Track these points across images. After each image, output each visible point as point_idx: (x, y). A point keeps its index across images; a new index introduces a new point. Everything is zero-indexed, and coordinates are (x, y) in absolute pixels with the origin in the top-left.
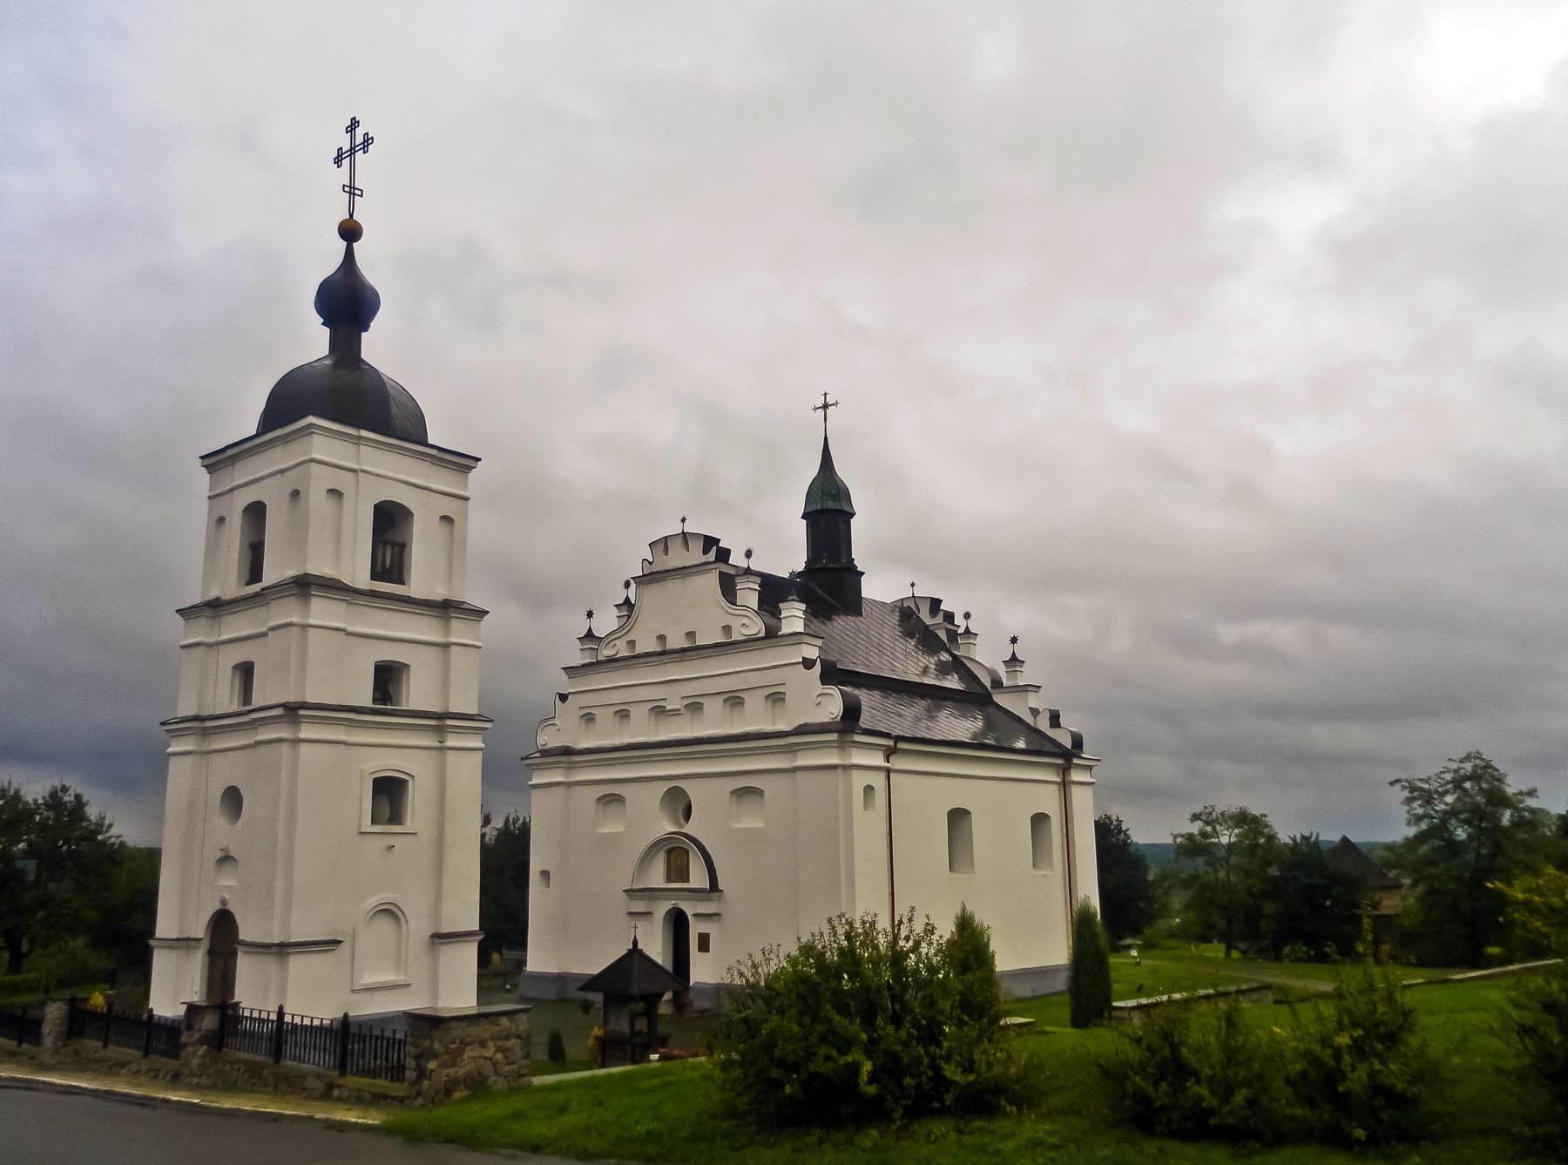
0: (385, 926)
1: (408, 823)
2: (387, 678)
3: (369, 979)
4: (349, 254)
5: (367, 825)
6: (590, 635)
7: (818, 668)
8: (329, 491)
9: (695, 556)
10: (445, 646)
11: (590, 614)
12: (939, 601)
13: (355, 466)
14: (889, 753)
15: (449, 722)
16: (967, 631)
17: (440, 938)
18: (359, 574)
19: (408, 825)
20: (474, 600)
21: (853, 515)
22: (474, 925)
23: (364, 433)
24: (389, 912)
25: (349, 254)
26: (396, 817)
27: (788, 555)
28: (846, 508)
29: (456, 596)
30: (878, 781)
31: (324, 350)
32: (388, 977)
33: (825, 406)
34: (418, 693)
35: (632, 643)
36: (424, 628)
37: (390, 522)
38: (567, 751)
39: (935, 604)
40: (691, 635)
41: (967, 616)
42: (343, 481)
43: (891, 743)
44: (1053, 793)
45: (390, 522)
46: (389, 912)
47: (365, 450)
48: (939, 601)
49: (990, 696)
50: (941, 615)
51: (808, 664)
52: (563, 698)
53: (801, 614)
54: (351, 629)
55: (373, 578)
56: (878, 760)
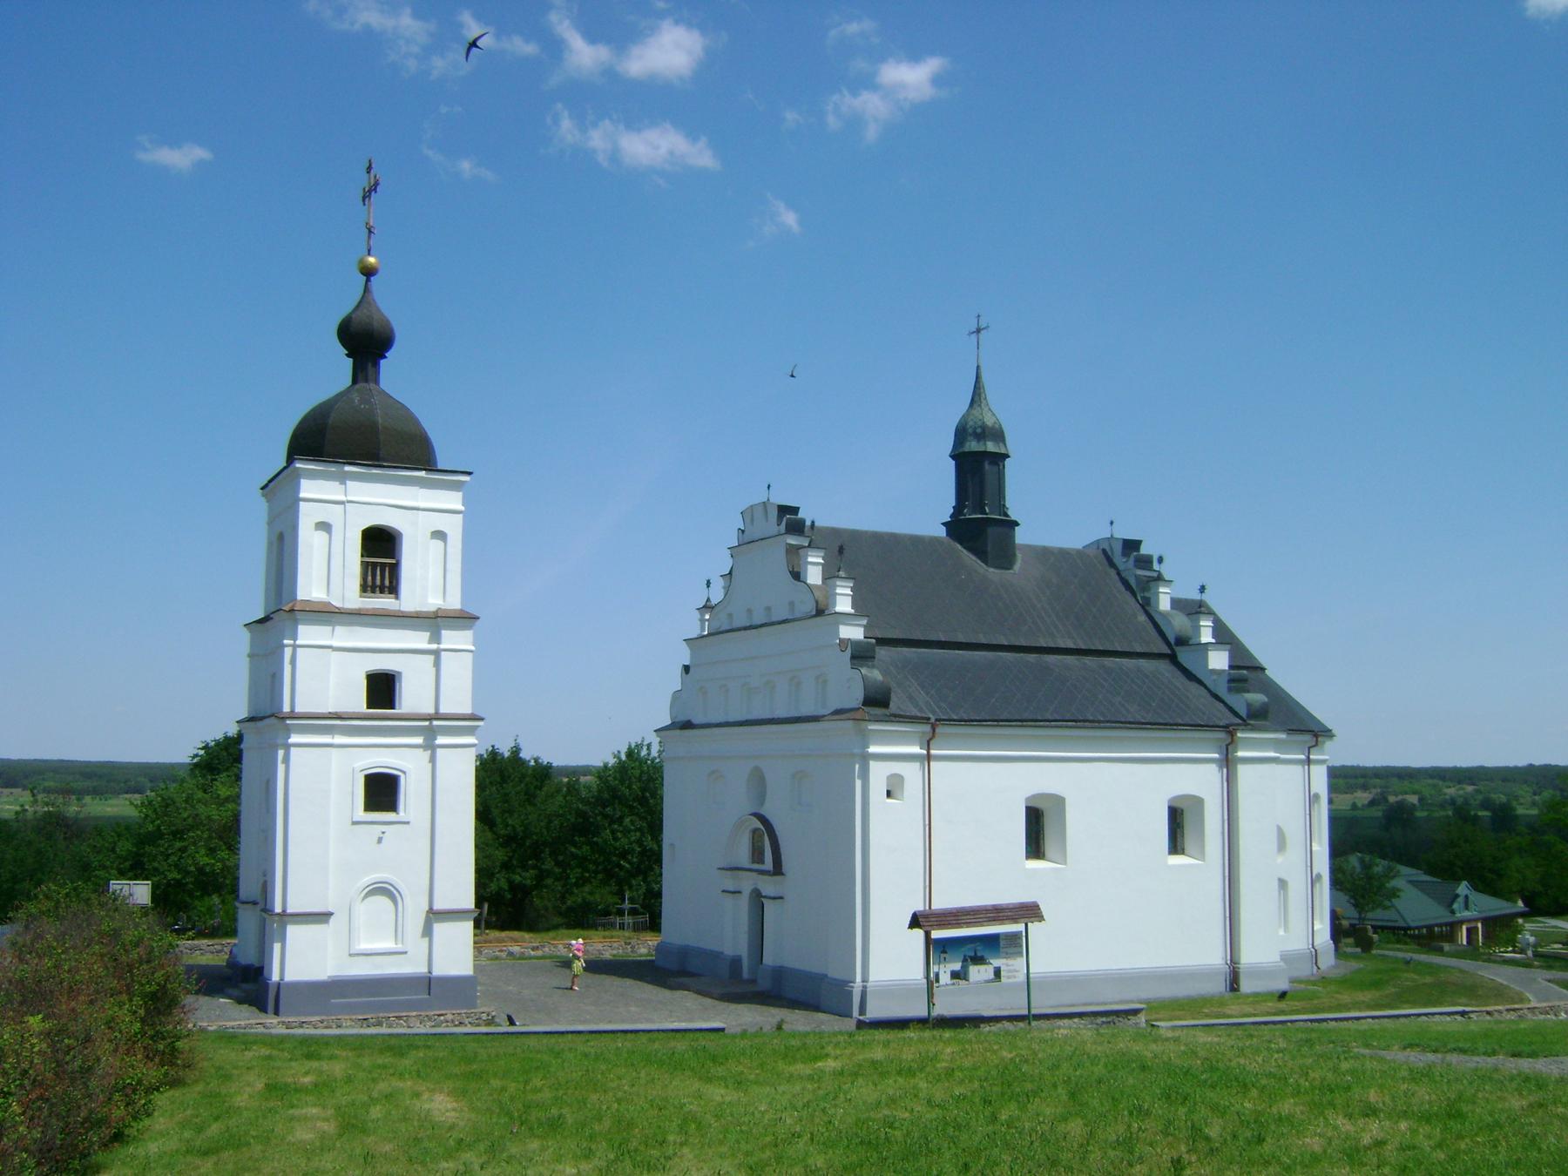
0: (382, 902)
1: (402, 813)
3: (364, 946)
4: (367, 289)
5: (360, 814)
6: (708, 607)
7: (848, 653)
9: (772, 525)
11: (708, 583)
13: (342, 498)
15: (435, 723)
16: (1159, 578)
17: (435, 915)
18: (349, 594)
19: (402, 815)
21: (1007, 456)
22: (467, 900)
23: (348, 468)
24: (383, 890)
27: (923, 504)
28: (991, 447)
30: (911, 772)
31: (347, 380)
32: (389, 945)
33: (978, 331)
34: (413, 696)
35: (730, 615)
36: (418, 639)
37: (380, 545)
38: (687, 725)
39: (1131, 546)
40: (768, 609)
41: (1160, 560)
42: (333, 514)
43: (927, 728)
45: (380, 545)
46: (383, 890)
51: (844, 643)
52: (687, 669)
53: (849, 592)
54: (335, 644)
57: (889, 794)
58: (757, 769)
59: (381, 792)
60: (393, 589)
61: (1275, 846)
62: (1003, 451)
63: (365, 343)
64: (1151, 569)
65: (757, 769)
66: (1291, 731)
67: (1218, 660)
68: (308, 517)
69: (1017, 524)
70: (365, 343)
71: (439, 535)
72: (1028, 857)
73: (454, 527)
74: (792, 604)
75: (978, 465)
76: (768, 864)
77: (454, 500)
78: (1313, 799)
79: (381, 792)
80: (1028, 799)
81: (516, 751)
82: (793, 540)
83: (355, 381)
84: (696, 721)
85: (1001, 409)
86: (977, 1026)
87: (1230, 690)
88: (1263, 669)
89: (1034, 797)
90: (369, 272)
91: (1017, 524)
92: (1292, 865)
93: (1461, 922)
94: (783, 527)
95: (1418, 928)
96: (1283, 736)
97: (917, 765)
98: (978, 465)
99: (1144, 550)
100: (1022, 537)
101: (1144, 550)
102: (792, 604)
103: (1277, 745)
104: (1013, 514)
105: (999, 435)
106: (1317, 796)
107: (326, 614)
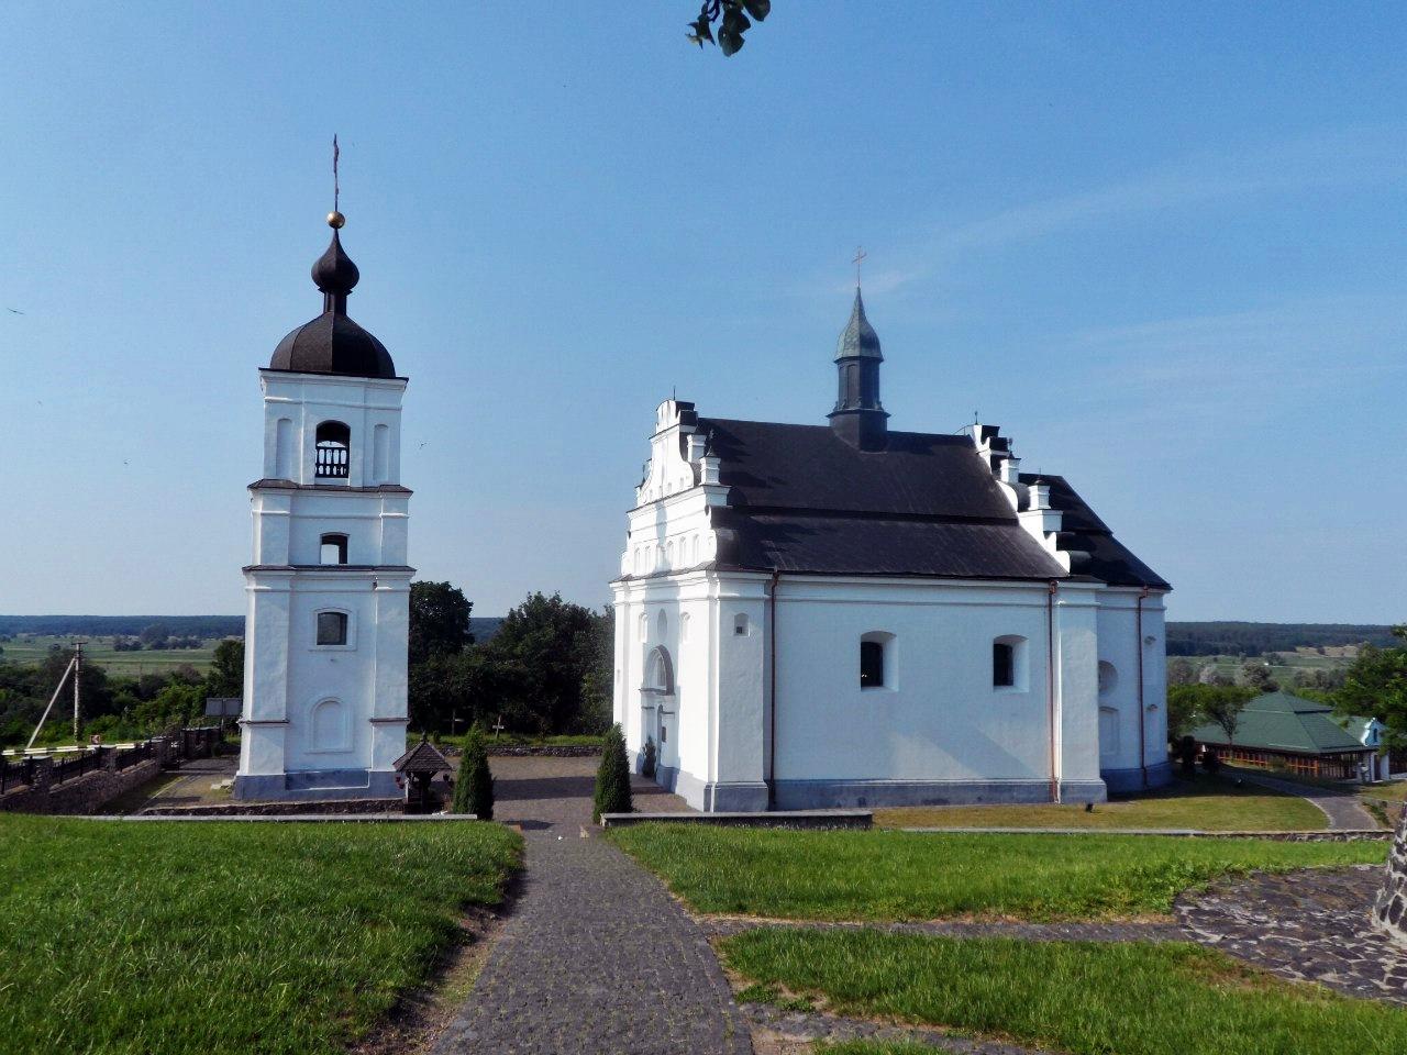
8: (280, 420)
12: (997, 428)
14: (772, 587)
20: (403, 484)
21: (882, 361)
25: (337, 235)
26: (342, 640)
28: (866, 353)
29: (385, 479)
41: (1011, 442)
43: (770, 577)
44: (1041, 614)
47: (304, 388)
48: (997, 428)
49: (1015, 522)
50: (988, 439)
55: (318, 475)
56: (759, 592)
57: (740, 630)
58: (662, 611)
59: (334, 629)
60: (343, 469)
61: (855, 674)
62: (875, 355)
64: (1005, 449)
65: (662, 611)
66: (1109, 585)
67: (1056, 522)
69: (889, 416)
72: (865, 683)
74: (682, 479)
75: (863, 366)
76: (664, 688)
78: (1142, 642)
80: (862, 636)
81: (557, 598)
82: (687, 429)
84: (634, 575)
85: (876, 322)
86: (772, 826)
87: (1059, 548)
88: (1108, 533)
89: (874, 633)
91: (889, 416)
92: (1125, 696)
93: (1369, 751)
94: (678, 421)
95: (1328, 754)
96: (1102, 586)
98: (863, 366)
99: (1001, 435)
100: (893, 425)
101: (1001, 435)
102: (682, 479)
103: (1098, 592)
104: (887, 410)
105: (869, 341)
106: (1151, 638)
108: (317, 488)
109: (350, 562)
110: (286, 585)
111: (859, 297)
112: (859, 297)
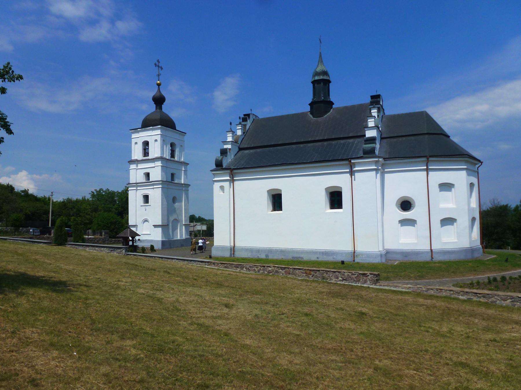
2: (148, 175)
10: (154, 167)
30: (226, 185)
37: (146, 144)
45: (146, 144)
46: (146, 221)
59: (146, 198)
63: (159, 101)
68: (133, 141)
70: (159, 101)
71: (156, 140)
73: (159, 138)
77: (159, 132)
79: (146, 198)
83: (156, 109)
90: (159, 85)
97: (228, 183)
107: (137, 162)
108: (142, 160)
109: (150, 180)
110: (135, 188)
111: (321, 56)
112: (321, 56)
